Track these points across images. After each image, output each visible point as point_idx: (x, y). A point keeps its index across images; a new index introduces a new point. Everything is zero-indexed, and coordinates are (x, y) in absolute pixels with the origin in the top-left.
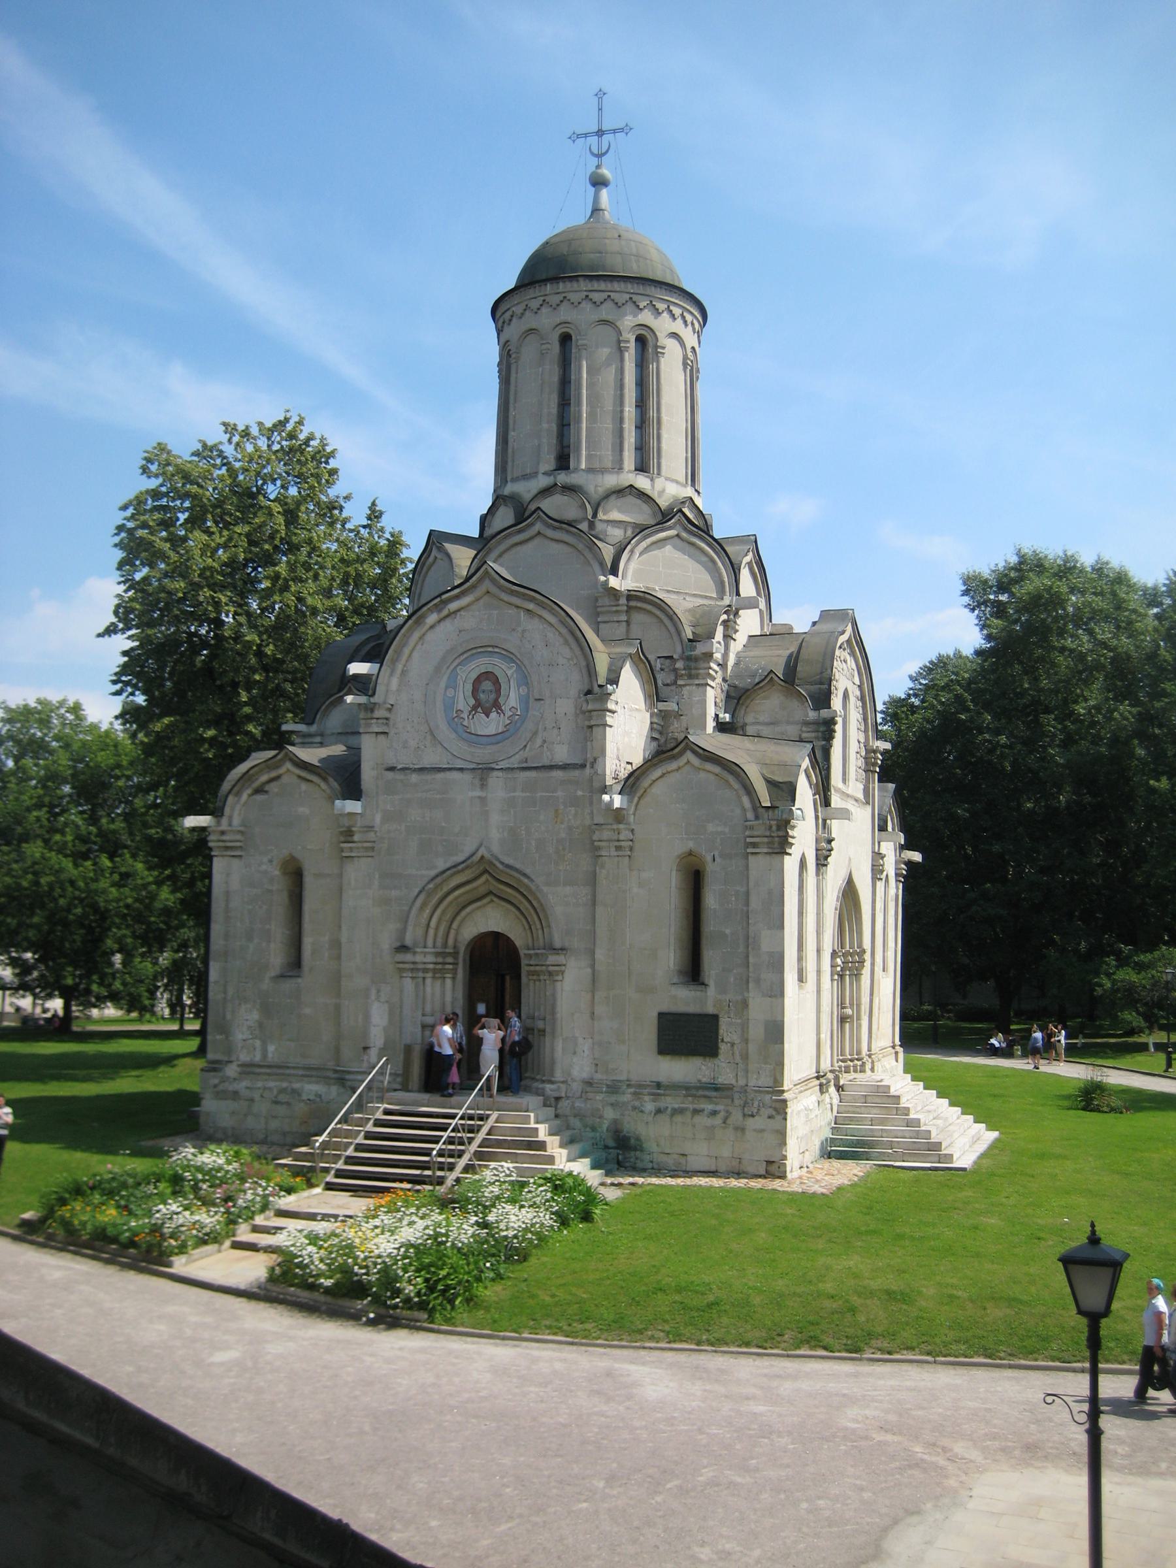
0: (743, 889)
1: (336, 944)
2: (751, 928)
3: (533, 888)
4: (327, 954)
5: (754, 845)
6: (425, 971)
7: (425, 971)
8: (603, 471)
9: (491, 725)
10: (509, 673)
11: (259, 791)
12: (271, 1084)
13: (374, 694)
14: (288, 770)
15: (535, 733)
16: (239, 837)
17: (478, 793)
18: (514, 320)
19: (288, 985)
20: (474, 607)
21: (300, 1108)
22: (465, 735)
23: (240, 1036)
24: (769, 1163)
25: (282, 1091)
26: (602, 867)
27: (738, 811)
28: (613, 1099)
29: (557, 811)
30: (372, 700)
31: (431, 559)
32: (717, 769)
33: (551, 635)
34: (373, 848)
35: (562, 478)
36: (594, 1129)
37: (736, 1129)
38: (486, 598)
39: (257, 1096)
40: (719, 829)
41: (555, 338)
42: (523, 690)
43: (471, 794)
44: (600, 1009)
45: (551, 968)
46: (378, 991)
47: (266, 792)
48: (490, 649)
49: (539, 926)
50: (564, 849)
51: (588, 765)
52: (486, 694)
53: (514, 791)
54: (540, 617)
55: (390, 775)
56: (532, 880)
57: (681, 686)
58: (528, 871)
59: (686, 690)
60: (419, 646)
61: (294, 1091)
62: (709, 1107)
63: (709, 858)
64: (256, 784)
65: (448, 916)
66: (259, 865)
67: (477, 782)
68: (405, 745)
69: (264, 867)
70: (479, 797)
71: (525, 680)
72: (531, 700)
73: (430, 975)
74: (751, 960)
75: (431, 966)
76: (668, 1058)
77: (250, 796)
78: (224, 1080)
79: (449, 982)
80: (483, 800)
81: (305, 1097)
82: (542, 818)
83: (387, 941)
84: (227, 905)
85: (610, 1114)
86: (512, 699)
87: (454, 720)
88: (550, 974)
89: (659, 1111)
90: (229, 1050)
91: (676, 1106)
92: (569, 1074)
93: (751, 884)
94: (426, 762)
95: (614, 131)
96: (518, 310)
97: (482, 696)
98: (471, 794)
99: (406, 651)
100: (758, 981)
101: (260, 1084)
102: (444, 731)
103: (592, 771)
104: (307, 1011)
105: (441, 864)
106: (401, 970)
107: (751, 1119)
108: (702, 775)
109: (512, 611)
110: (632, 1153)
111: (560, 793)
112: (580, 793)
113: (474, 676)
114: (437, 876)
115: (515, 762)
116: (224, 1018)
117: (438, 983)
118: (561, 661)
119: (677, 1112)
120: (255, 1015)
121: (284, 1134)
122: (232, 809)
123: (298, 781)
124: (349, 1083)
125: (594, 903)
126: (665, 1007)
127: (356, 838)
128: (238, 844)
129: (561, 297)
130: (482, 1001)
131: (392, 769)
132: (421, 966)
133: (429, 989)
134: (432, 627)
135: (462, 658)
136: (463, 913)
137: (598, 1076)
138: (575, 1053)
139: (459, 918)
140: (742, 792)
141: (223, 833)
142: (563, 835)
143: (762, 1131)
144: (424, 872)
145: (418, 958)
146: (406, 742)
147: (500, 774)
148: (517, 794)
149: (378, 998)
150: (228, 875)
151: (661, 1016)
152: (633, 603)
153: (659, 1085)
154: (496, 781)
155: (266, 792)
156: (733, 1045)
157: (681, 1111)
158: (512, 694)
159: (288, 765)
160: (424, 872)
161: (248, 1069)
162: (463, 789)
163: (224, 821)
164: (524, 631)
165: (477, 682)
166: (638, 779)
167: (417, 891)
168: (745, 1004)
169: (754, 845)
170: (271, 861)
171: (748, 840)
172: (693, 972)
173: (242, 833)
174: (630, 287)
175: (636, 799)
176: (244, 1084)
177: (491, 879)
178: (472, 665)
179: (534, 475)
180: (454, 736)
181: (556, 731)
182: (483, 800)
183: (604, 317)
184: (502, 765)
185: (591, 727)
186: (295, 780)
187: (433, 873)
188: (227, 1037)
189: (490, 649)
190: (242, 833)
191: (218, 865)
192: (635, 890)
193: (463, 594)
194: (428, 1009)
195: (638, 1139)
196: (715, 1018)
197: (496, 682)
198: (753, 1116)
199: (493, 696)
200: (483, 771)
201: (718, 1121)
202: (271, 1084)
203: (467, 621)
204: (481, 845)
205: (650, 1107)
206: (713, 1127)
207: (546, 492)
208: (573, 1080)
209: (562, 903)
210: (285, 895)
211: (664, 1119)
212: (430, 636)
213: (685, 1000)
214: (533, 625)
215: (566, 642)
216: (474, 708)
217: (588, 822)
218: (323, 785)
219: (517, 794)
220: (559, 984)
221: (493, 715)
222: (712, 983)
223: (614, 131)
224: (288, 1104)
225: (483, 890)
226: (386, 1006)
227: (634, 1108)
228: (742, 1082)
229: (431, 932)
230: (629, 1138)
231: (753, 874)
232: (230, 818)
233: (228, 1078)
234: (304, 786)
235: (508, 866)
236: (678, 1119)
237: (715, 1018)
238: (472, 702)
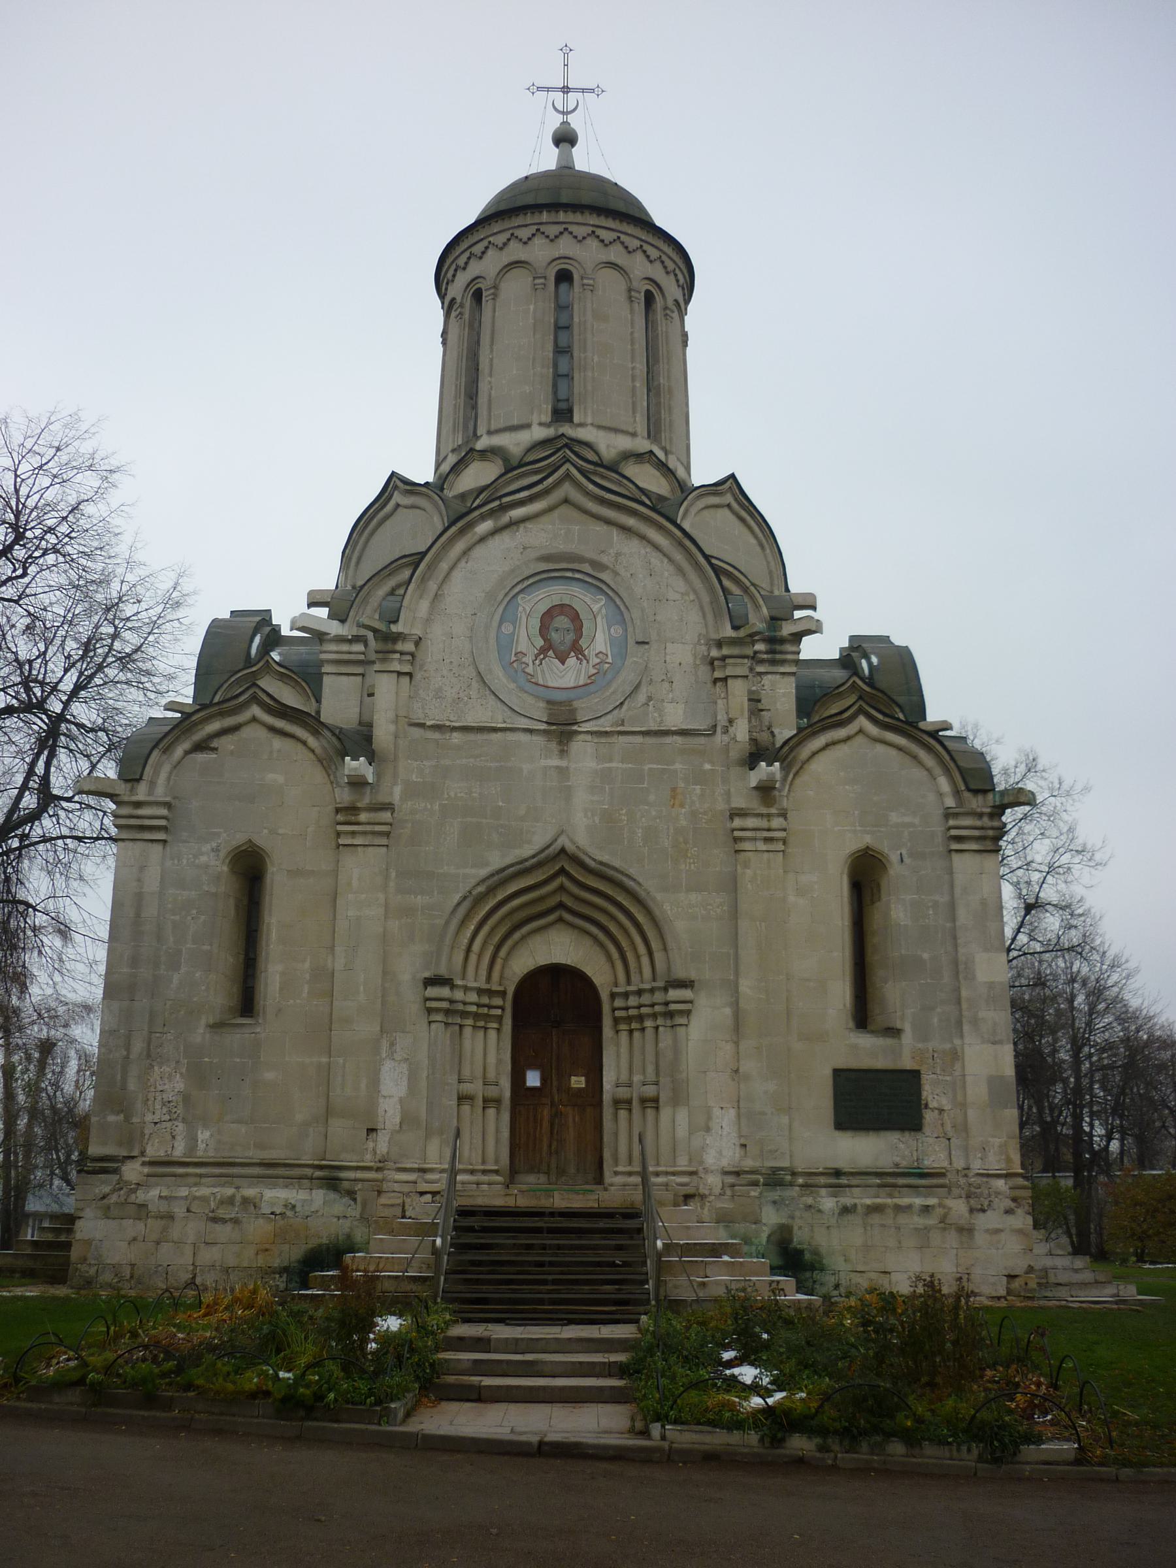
0: (943, 899)
1: (324, 979)
2: (961, 950)
3: (643, 894)
4: (306, 988)
5: (959, 839)
6: (464, 1014)
7: (464, 1014)
8: (616, 430)
10: (595, 608)
11: (200, 747)
12: (204, 1191)
13: (396, 622)
14: (254, 719)
15: (637, 687)
16: (164, 812)
17: (555, 762)
18: (490, 252)
19: (234, 1039)
20: (545, 519)
21: (257, 1228)
22: (528, 687)
23: (149, 1118)
24: (1011, 1277)
25: (230, 1201)
26: (746, 865)
27: (932, 797)
28: (775, 1194)
29: (674, 790)
30: (394, 628)
31: (390, 507)
32: (901, 741)
33: (656, 559)
34: (387, 834)
37: (961, 1230)
38: (564, 510)
39: (179, 1210)
40: (907, 819)
42: (617, 631)
43: (544, 762)
44: (748, 1066)
45: (673, 1007)
46: (392, 1044)
47: (215, 749)
48: (569, 574)
49: (642, 949)
50: (686, 842)
51: (719, 729)
52: (561, 634)
53: (611, 761)
54: (643, 537)
55: (416, 732)
56: (639, 884)
57: (760, 674)
58: (632, 871)
59: (767, 680)
60: (462, 564)
61: (246, 1201)
62: (918, 1201)
63: (894, 858)
64: (198, 736)
65: (496, 939)
66: (195, 857)
67: (553, 745)
68: (439, 694)
69: (204, 859)
70: (557, 767)
72: (631, 642)
73: (470, 1022)
74: (964, 993)
75: (474, 1009)
76: (849, 1134)
77: (187, 753)
78: (120, 1185)
79: (492, 1034)
80: (563, 772)
81: (266, 1210)
82: (652, 798)
83: (409, 968)
84: (138, 915)
85: (771, 1218)
86: (599, 641)
87: (513, 665)
88: (670, 1015)
90: (132, 1136)
91: (868, 1202)
92: (701, 1162)
93: (958, 891)
94: (470, 721)
95: (583, 90)
96: (500, 239)
97: (555, 636)
98: (544, 762)
99: (444, 566)
100: (975, 1022)
101: (184, 1192)
103: (726, 738)
104: (270, 1076)
106: (430, 1011)
107: (981, 1215)
108: (880, 748)
109: (601, 528)
110: (808, 1274)
111: (678, 766)
112: (707, 766)
113: (543, 608)
114: (492, 875)
115: (605, 725)
116: (124, 1087)
117: (481, 1033)
118: (672, 595)
120: (179, 1084)
121: (227, 1271)
122: (156, 773)
123: (270, 735)
124: (346, 1185)
125: (734, 913)
126: (841, 1064)
128: (163, 822)
129: (561, 228)
130: (533, 1067)
131: (422, 725)
132: (461, 1007)
133: (467, 1043)
134: (482, 539)
135: (527, 583)
136: (517, 936)
137: (749, 1164)
138: (708, 1129)
139: (510, 942)
140: (938, 771)
141: (138, 805)
142: (683, 823)
143: (998, 1231)
144: (467, 871)
145: (459, 995)
146: (440, 689)
147: (589, 737)
148: (614, 765)
149: (391, 1056)
150: (142, 868)
151: (837, 1072)
153: (838, 1173)
155: (215, 749)
156: (941, 1111)
158: (600, 637)
159: (256, 710)
160: (467, 871)
163: (142, 788)
164: (618, 555)
165: (548, 616)
166: (792, 750)
167: (457, 898)
168: (955, 1056)
169: (959, 839)
170: (216, 850)
171: (954, 832)
172: (863, 1013)
173: (168, 805)
175: (791, 776)
176: (155, 1193)
177: (568, 885)
179: (528, 426)
180: (512, 686)
181: (666, 685)
182: (563, 772)
183: (612, 258)
185: (725, 680)
186: (262, 733)
187: (483, 872)
188: (127, 1119)
189: (569, 574)
190: (168, 805)
192: (792, 898)
194: (466, 1073)
195: (816, 1253)
196: (915, 1075)
197: (575, 618)
198: (984, 1211)
199: (570, 637)
201: (932, 1221)
202: (204, 1191)
204: (561, 832)
206: (927, 1229)
208: (706, 1170)
209: (686, 914)
210: (232, 902)
211: (855, 1219)
212: (478, 551)
213: (868, 1052)
214: (632, 547)
215: (680, 571)
216: (543, 651)
217: (721, 806)
218: (312, 741)
219: (614, 765)
220: (682, 1030)
221: (572, 661)
222: (907, 1028)
223: (583, 90)
224: (236, 1221)
225: (552, 902)
226: (405, 1066)
227: (809, 1207)
228: (959, 1164)
229: (473, 958)
230: (800, 1252)
231: (959, 879)
232: (152, 784)
233: (128, 1183)
234: (278, 743)
235: (601, 863)
236: (876, 1219)
237: (915, 1075)
238: (540, 642)
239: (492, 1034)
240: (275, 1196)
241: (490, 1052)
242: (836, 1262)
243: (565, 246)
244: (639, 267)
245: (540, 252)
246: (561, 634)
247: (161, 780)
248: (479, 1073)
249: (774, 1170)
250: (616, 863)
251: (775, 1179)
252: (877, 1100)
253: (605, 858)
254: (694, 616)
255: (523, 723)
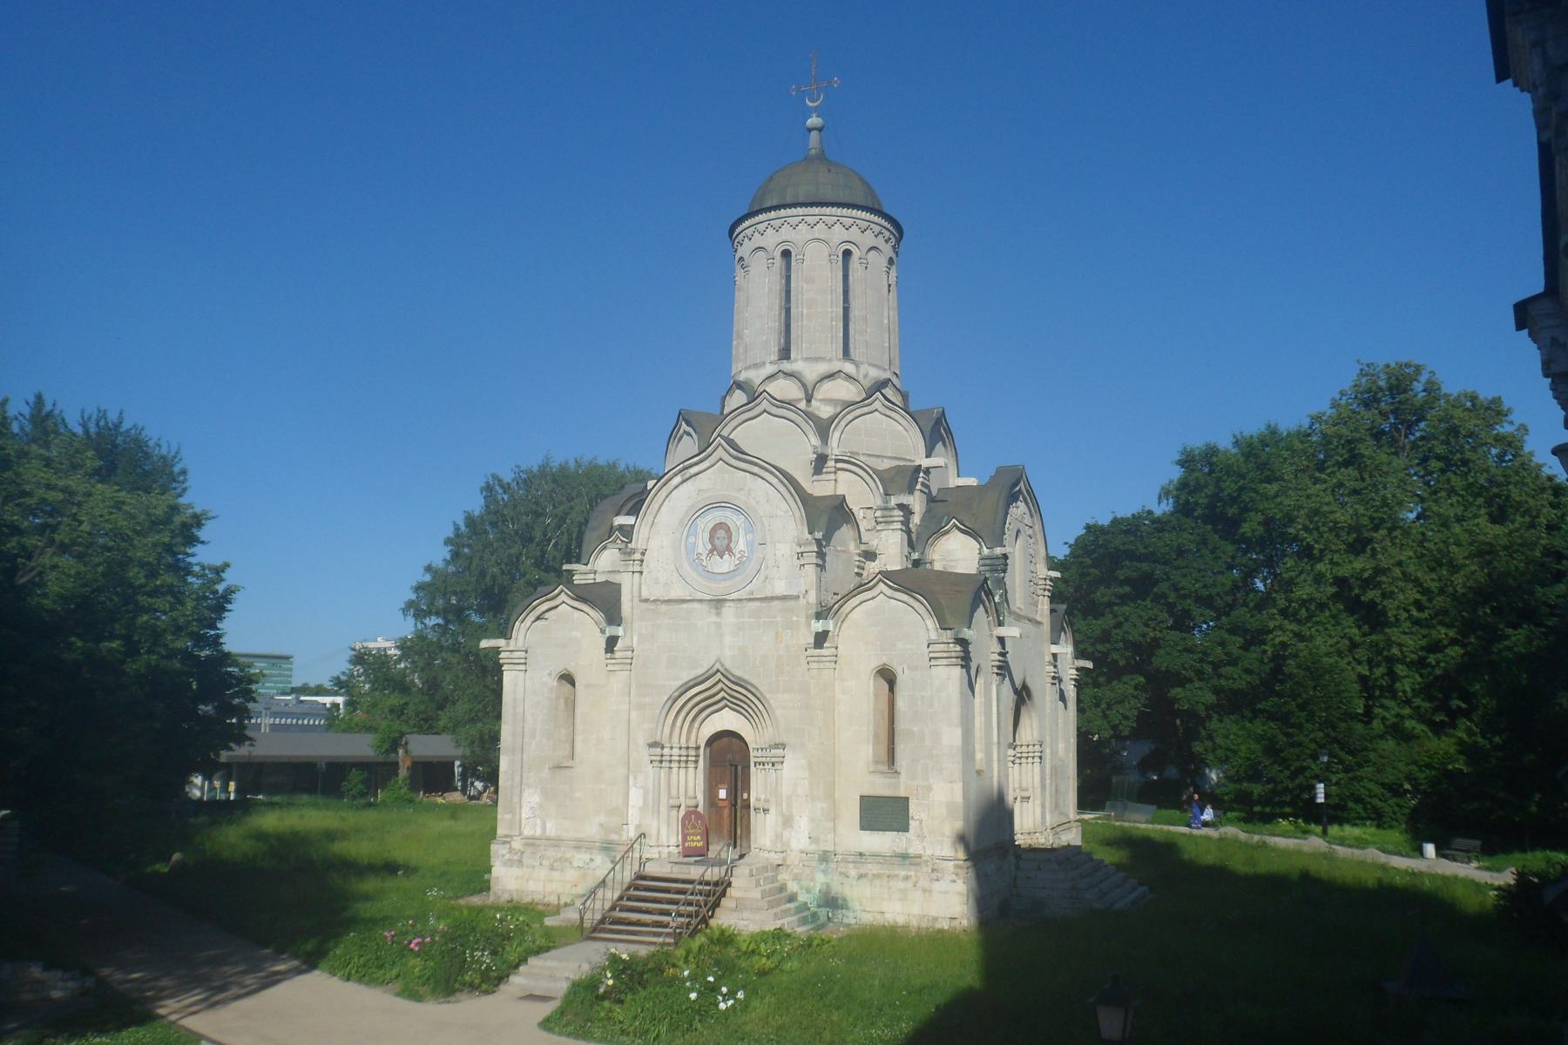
8: (817, 359)
9: (724, 564)
11: (538, 618)
17: (714, 619)
21: (571, 875)
35: (786, 366)
36: (808, 891)
37: (924, 890)
41: (778, 254)
52: (721, 540)
55: (644, 605)
62: (903, 873)
71: (751, 529)
79: (691, 770)
83: (641, 738)
85: (821, 879)
86: (740, 545)
89: (860, 877)
94: (674, 595)
97: (717, 542)
102: (687, 569)
104: (578, 795)
105: (686, 676)
115: (743, 594)
118: (780, 513)
119: (877, 876)
127: (618, 655)
136: (704, 715)
137: (813, 847)
140: (926, 615)
143: (946, 893)
152: (840, 465)
153: (861, 854)
154: (729, 611)
157: (877, 876)
161: (531, 842)
162: (704, 617)
163: (512, 642)
168: (929, 789)
174: (834, 210)
178: (709, 517)
182: (719, 625)
184: (733, 596)
191: (508, 677)
193: (701, 461)
195: (844, 900)
197: (728, 530)
200: (718, 603)
201: (909, 884)
203: (704, 481)
205: (853, 872)
207: (771, 377)
209: (782, 704)
213: (881, 787)
216: (711, 552)
221: (726, 556)
222: (903, 771)
236: (877, 882)
239: (691, 770)
240: (580, 858)
241: (692, 783)
242: (855, 904)
243: (786, 234)
244: (839, 234)
245: (771, 239)
246: (721, 540)
247: (521, 637)
248: (682, 790)
249: (825, 852)
250: (746, 677)
251: (825, 857)
252: (884, 813)
253: (739, 673)
254: (792, 525)
255: (700, 596)
